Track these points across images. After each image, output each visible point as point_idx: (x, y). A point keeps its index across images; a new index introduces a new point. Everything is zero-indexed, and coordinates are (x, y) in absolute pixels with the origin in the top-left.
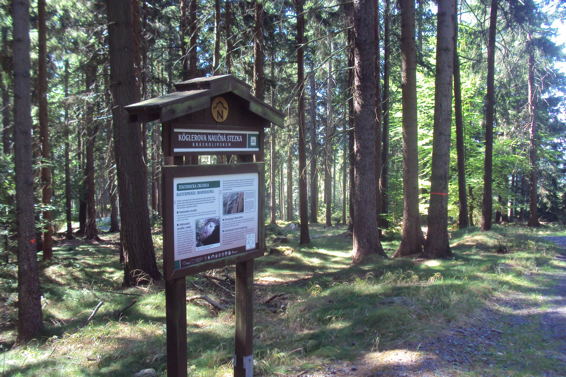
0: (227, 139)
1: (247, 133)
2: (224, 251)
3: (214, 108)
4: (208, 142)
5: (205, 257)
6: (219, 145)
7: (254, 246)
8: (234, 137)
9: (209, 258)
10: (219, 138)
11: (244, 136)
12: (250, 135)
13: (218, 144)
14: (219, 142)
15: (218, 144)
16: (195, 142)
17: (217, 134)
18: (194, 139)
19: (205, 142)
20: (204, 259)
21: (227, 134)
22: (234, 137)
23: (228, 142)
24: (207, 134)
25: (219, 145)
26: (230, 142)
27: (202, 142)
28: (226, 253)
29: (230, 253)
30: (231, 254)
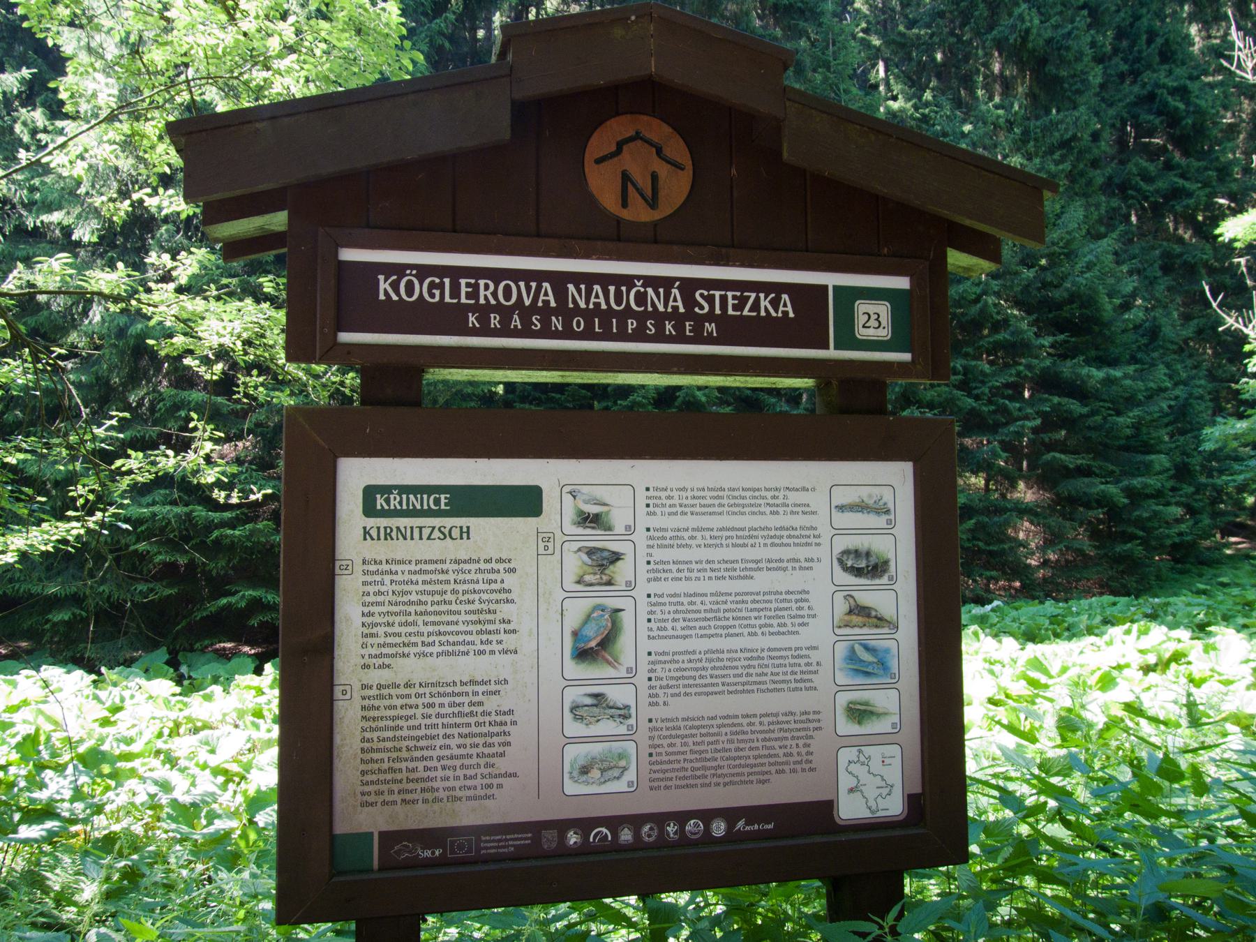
0: (690, 302)
3: (599, 161)
4: (567, 313)
6: (642, 327)
8: (742, 301)
9: (573, 838)
11: (810, 297)
12: (848, 296)
13: (632, 325)
14: (641, 318)
15: (632, 325)
16: (484, 311)
17: (628, 280)
18: (474, 294)
19: (546, 312)
21: (688, 286)
22: (742, 301)
23: (700, 321)
24: (559, 280)
25: (642, 327)
26: (710, 317)
27: (526, 313)
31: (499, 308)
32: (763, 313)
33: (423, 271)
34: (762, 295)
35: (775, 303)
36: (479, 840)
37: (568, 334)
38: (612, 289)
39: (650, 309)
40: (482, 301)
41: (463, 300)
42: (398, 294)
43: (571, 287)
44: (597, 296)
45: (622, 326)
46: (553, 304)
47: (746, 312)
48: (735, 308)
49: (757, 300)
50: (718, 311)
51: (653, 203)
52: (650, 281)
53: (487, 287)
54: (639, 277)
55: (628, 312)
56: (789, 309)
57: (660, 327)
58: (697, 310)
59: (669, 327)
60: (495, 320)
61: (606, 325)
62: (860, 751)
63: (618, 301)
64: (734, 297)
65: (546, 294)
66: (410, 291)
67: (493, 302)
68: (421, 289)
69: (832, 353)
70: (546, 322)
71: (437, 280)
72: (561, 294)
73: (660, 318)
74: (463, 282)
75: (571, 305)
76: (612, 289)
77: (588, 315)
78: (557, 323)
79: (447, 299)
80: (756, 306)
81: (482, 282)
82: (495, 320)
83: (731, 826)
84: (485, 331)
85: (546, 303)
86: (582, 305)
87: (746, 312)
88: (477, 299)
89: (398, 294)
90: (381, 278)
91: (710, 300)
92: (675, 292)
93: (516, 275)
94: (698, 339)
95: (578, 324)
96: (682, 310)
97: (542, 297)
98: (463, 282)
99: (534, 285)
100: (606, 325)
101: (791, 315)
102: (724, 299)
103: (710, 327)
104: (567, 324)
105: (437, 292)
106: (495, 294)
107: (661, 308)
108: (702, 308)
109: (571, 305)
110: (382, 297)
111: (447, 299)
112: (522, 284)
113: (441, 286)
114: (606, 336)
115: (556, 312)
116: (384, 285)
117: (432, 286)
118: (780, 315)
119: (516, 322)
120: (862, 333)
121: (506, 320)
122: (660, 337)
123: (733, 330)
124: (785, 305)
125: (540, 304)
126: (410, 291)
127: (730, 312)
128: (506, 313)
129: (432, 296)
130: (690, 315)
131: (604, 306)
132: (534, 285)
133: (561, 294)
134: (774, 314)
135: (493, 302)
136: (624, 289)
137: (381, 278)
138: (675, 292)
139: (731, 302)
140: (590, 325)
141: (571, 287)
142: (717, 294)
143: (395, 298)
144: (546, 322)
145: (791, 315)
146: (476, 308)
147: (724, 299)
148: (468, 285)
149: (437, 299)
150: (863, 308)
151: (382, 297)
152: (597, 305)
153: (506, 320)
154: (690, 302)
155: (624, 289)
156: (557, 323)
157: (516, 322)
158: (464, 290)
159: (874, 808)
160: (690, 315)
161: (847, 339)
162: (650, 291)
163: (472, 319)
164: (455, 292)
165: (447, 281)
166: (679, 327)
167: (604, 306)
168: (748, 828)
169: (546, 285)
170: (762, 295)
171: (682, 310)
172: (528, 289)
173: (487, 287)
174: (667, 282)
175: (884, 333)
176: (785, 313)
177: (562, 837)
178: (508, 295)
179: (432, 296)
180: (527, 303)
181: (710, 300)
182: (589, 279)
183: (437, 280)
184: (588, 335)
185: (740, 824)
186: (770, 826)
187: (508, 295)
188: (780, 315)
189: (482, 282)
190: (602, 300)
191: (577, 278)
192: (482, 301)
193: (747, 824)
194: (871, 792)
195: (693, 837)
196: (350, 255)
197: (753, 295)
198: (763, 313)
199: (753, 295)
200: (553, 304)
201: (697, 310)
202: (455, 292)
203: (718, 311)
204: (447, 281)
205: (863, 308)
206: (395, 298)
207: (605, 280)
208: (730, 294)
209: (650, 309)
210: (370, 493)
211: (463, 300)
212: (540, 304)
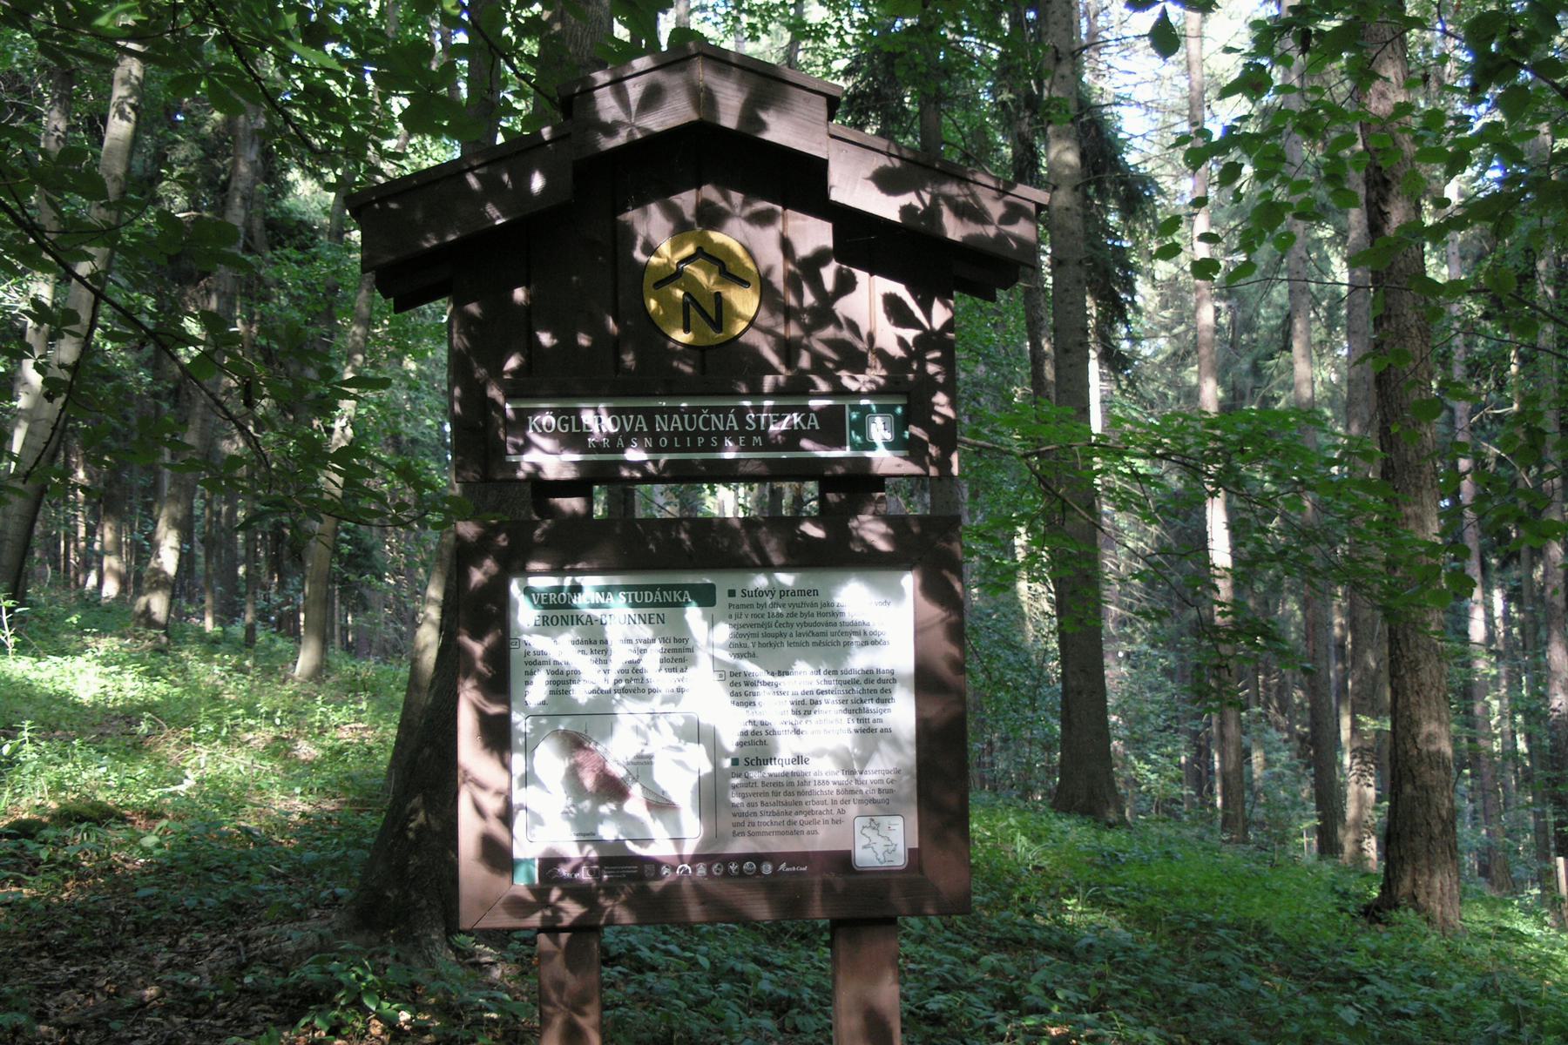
7: (900, 861)
10: (707, 422)
13: (701, 440)
14: (708, 435)
15: (701, 440)
28: (747, 865)
29: (767, 868)
45: (694, 442)
52: (712, 410)
55: (698, 432)
61: (682, 441)
63: (691, 425)
72: (651, 423)
77: (671, 435)
85: (641, 429)
103: (757, 440)
113: (569, 422)
117: (563, 421)
130: (742, 431)
133: (651, 423)
140: (671, 442)
160: (742, 431)
174: (726, 410)
191: (661, 411)
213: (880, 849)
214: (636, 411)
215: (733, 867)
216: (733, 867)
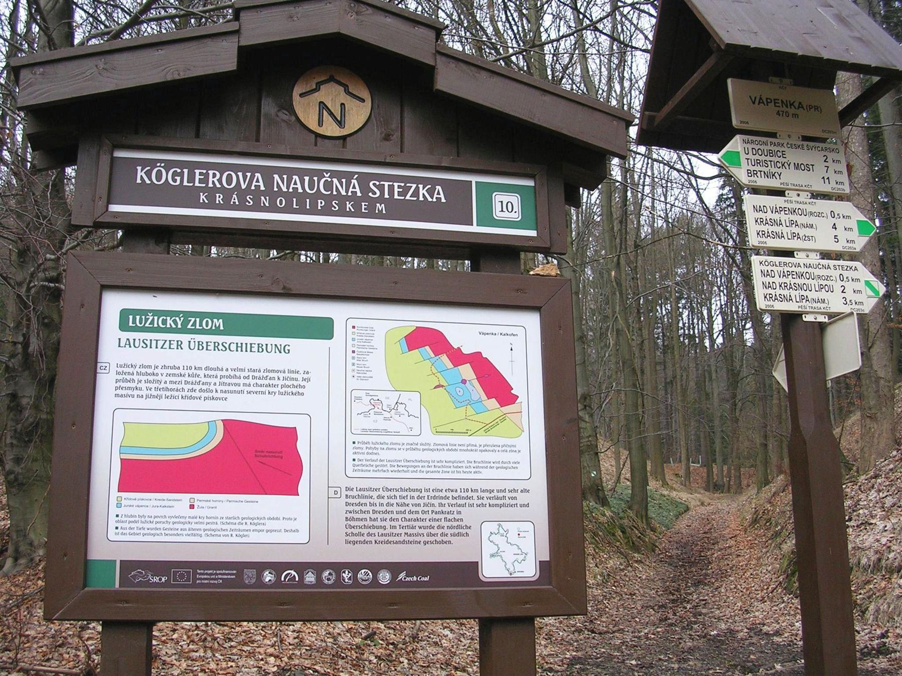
0: (365, 189)
1: (474, 179)
2: (355, 567)
3: (301, 95)
4: (273, 195)
5: (250, 573)
10: (328, 186)
13: (321, 204)
14: (329, 199)
15: (321, 204)
16: (211, 192)
17: (320, 174)
18: (205, 180)
19: (257, 193)
20: (240, 575)
21: (364, 180)
22: (405, 190)
23: (372, 203)
24: (268, 174)
26: (381, 199)
27: (242, 194)
28: (361, 575)
29: (385, 577)
30: (393, 582)
31: (223, 190)
32: (421, 199)
33: (169, 165)
34: (421, 186)
35: (431, 192)
36: (195, 573)
37: (273, 209)
38: (307, 179)
39: (335, 193)
40: (211, 185)
41: (197, 184)
42: (150, 179)
43: (276, 177)
44: (295, 183)
45: (314, 204)
46: (262, 188)
47: (408, 197)
48: (399, 194)
49: (417, 189)
50: (386, 196)
51: (340, 123)
52: (334, 174)
53: (214, 175)
54: (327, 171)
55: (318, 194)
56: (442, 196)
57: (342, 206)
58: (370, 194)
59: (348, 206)
60: (219, 198)
61: (302, 203)
62: (499, 525)
63: (311, 187)
64: (399, 187)
65: (258, 181)
66: (159, 177)
67: (218, 186)
68: (167, 176)
69: (475, 228)
70: (257, 201)
71: (179, 171)
72: (269, 182)
73: (342, 200)
74: (197, 172)
75: (276, 189)
76: (307, 179)
77: (288, 196)
78: (265, 201)
79: (185, 183)
80: (416, 193)
81: (211, 172)
82: (219, 198)
83: (394, 576)
84: (212, 205)
85: (258, 187)
86: (284, 189)
87: (408, 197)
88: (208, 184)
89: (150, 179)
90: (139, 168)
91: (381, 188)
92: (354, 181)
93: (236, 168)
94: (371, 215)
95: (281, 202)
96: (359, 194)
97: (254, 183)
98: (197, 172)
99: (249, 174)
100: (302, 203)
101: (443, 200)
102: (391, 188)
103: (380, 207)
104: (273, 202)
105: (178, 179)
106: (220, 181)
107: (343, 193)
108: (375, 193)
109: (276, 189)
110: (139, 181)
111: (185, 183)
112: (240, 174)
113: (181, 175)
114: (302, 211)
115: (264, 193)
116: (140, 173)
117: (175, 174)
118: (435, 200)
119: (235, 199)
120: (498, 214)
121: (227, 199)
122: (342, 213)
123: (396, 210)
124: (438, 193)
125: (253, 188)
126: (159, 177)
127: (396, 197)
128: (227, 194)
129: (175, 181)
131: (300, 190)
132: (249, 174)
133: (269, 182)
134: (430, 199)
135: (218, 186)
136: (316, 179)
137: (139, 168)
138: (354, 181)
139: (396, 190)
141: (276, 177)
142: (386, 184)
143: (148, 182)
144: (257, 201)
145: (443, 200)
146: (205, 190)
147: (391, 188)
148: (200, 174)
149: (178, 183)
150: (499, 198)
151: (139, 181)
152: (296, 189)
153: (227, 199)
154: (365, 189)
155: (316, 179)
156: (265, 201)
157: (235, 199)
158: (197, 177)
159: (512, 570)
160: (365, 197)
161: (487, 218)
162: (335, 180)
163: (202, 197)
164: (191, 179)
165: (186, 171)
166: (357, 206)
167: (300, 190)
168: (408, 579)
169: (258, 175)
170: (421, 186)
171: (359, 194)
172: (245, 178)
173: (214, 175)
174: (349, 176)
175: (516, 216)
176: (439, 199)
177: (260, 576)
178: (229, 181)
179: (175, 181)
180: (243, 187)
181: (381, 188)
182: (290, 172)
183: (179, 171)
184: (288, 210)
185: (402, 575)
186: (426, 579)
187: (229, 181)
188: (435, 200)
189: (211, 172)
190: (299, 186)
191: (281, 171)
192: (211, 185)
193: (407, 576)
194: (509, 557)
195: (364, 583)
196: (120, 154)
197: (414, 186)
198: (421, 199)
199: (414, 186)
200: (262, 188)
201: (370, 194)
202: (191, 179)
203: (386, 196)
204: (186, 171)
205: (499, 198)
206: (148, 182)
207: (302, 173)
208: (396, 185)
209: (335, 193)
210: (125, 314)
211: (197, 184)
212: (253, 188)
213: (509, 557)
214: (254, 169)
215: (346, 575)
216: (346, 575)
